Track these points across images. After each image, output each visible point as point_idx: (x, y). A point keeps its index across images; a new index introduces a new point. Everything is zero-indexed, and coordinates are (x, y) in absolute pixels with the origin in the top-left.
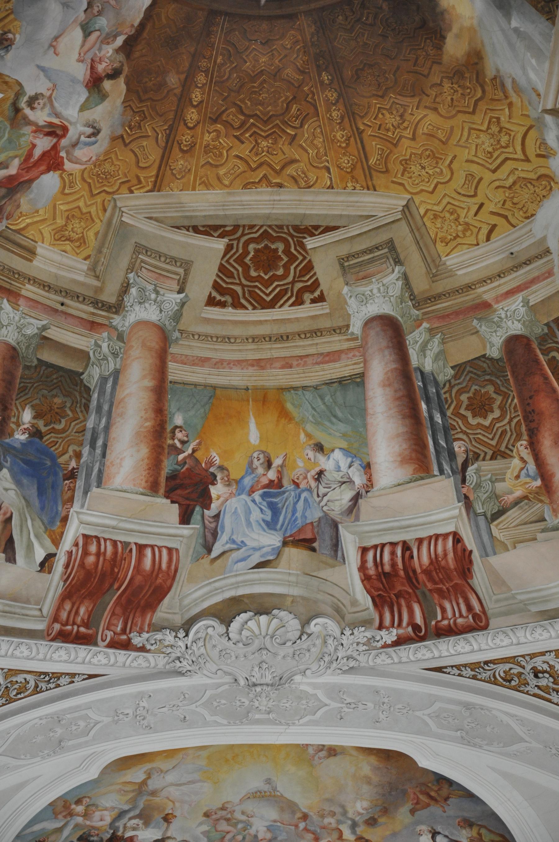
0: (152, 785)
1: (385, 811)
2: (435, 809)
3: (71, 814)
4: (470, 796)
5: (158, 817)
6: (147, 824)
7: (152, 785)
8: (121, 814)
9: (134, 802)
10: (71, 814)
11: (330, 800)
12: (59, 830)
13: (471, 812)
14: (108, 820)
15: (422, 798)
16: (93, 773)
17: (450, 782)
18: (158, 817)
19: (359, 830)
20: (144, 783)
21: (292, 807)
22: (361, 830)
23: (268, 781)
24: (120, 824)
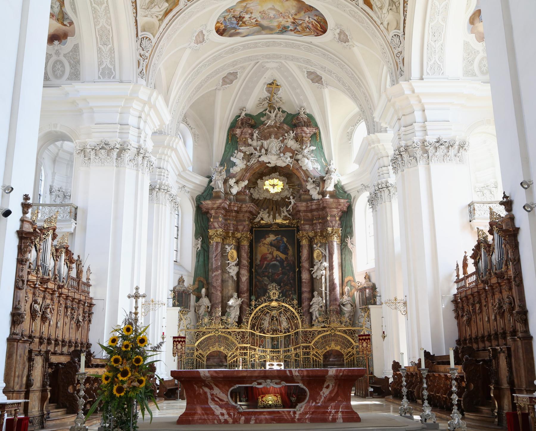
0: (247, 6)
1: (299, 12)
2: (309, 12)
3: (230, 12)
4: (317, 10)
5: (249, 13)
6: (247, 14)
7: (247, 6)
8: (241, 12)
9: (244, 9)
10: (230, 12)
11: (286, 10)
12: (228, 15)
13: (316, 13)
14: (239, 13)
15: (307, 10)
16: (235, 4)
17: (313, 7)
18: (249, 13)
19: (293, 16)
20: (246, 6)
21: (278, 11)
22: (293, 16)
23: (273, 6)
24: (241, 14)
